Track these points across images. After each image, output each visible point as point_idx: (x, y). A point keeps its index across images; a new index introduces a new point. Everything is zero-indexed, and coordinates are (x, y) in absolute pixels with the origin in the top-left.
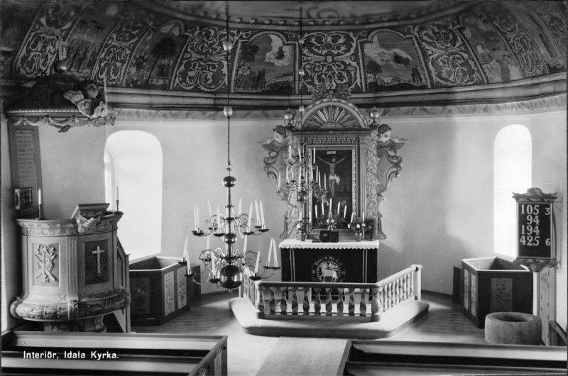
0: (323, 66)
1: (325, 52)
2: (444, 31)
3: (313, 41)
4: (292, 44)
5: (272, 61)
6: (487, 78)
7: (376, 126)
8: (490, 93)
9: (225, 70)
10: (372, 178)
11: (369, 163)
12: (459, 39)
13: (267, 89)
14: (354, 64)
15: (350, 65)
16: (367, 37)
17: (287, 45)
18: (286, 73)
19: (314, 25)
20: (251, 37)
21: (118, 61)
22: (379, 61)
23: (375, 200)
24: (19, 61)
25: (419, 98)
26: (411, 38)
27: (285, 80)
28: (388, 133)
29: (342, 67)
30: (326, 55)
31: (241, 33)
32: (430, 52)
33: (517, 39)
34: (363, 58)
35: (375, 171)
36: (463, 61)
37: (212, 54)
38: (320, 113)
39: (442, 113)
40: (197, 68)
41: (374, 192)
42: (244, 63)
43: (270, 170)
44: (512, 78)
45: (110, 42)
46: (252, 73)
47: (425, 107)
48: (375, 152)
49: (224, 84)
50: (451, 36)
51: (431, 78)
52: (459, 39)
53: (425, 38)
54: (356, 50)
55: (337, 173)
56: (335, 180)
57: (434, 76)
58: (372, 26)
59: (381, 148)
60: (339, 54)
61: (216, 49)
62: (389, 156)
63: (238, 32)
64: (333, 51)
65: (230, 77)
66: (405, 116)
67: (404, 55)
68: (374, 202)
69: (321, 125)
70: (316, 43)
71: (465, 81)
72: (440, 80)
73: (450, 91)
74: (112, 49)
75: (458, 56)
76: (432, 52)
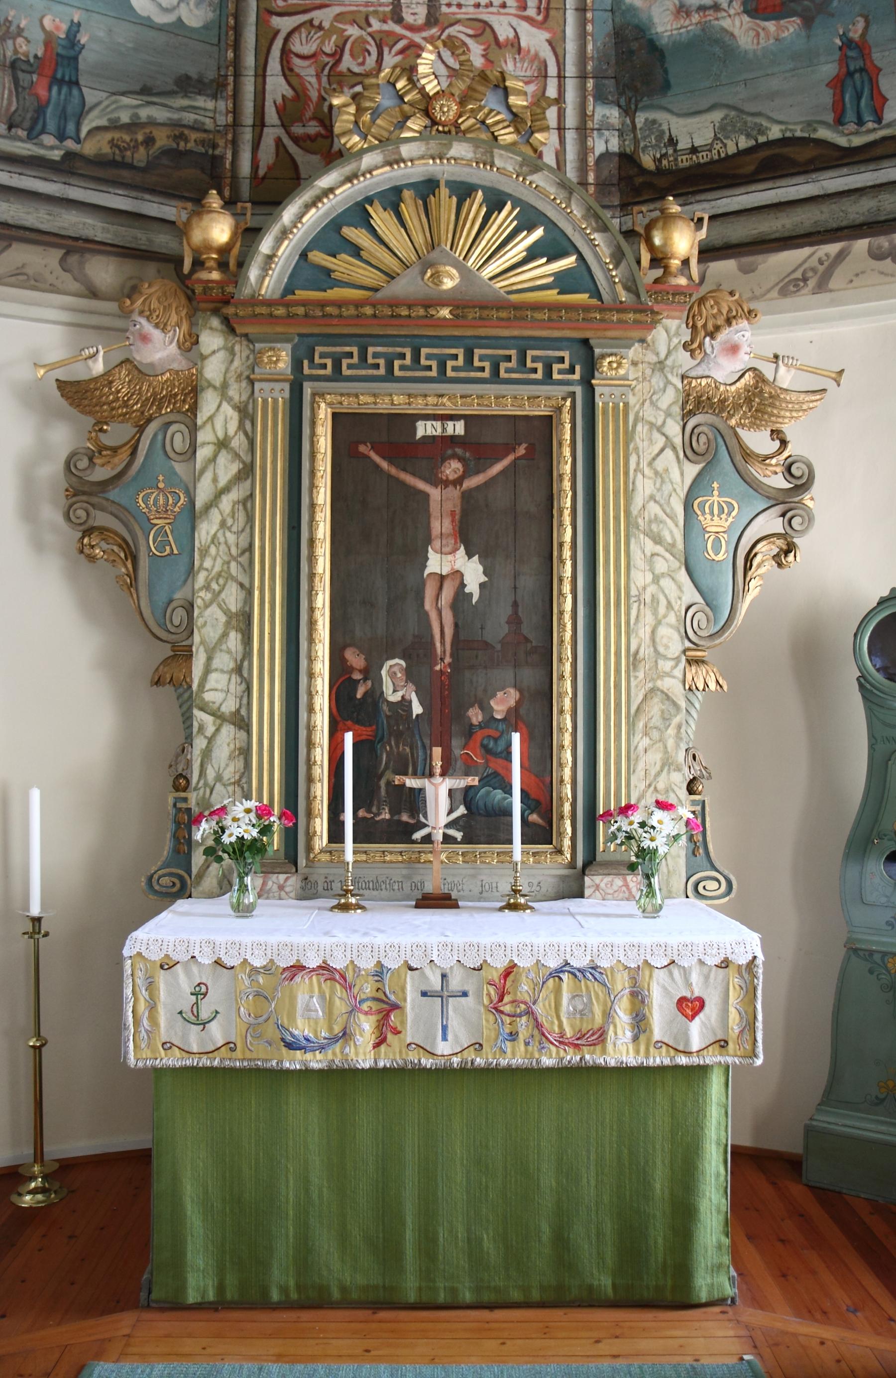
0: (382, 42)
7: (678, 292)
10: (661, 566)
11: (644, 487)
13: (89, 148)
15: (515, 45)
18: (193, 73)
23: (673, 686)
27: (189, 117)
29: (476, 55)
35: (674, 532)
38: (381, 218)
41: (673, 643)
43: (101, 519)
48: (674, 429)
56: (458, 574)
62: (748, 455)
66: (788, 301)
69: (391, 276)
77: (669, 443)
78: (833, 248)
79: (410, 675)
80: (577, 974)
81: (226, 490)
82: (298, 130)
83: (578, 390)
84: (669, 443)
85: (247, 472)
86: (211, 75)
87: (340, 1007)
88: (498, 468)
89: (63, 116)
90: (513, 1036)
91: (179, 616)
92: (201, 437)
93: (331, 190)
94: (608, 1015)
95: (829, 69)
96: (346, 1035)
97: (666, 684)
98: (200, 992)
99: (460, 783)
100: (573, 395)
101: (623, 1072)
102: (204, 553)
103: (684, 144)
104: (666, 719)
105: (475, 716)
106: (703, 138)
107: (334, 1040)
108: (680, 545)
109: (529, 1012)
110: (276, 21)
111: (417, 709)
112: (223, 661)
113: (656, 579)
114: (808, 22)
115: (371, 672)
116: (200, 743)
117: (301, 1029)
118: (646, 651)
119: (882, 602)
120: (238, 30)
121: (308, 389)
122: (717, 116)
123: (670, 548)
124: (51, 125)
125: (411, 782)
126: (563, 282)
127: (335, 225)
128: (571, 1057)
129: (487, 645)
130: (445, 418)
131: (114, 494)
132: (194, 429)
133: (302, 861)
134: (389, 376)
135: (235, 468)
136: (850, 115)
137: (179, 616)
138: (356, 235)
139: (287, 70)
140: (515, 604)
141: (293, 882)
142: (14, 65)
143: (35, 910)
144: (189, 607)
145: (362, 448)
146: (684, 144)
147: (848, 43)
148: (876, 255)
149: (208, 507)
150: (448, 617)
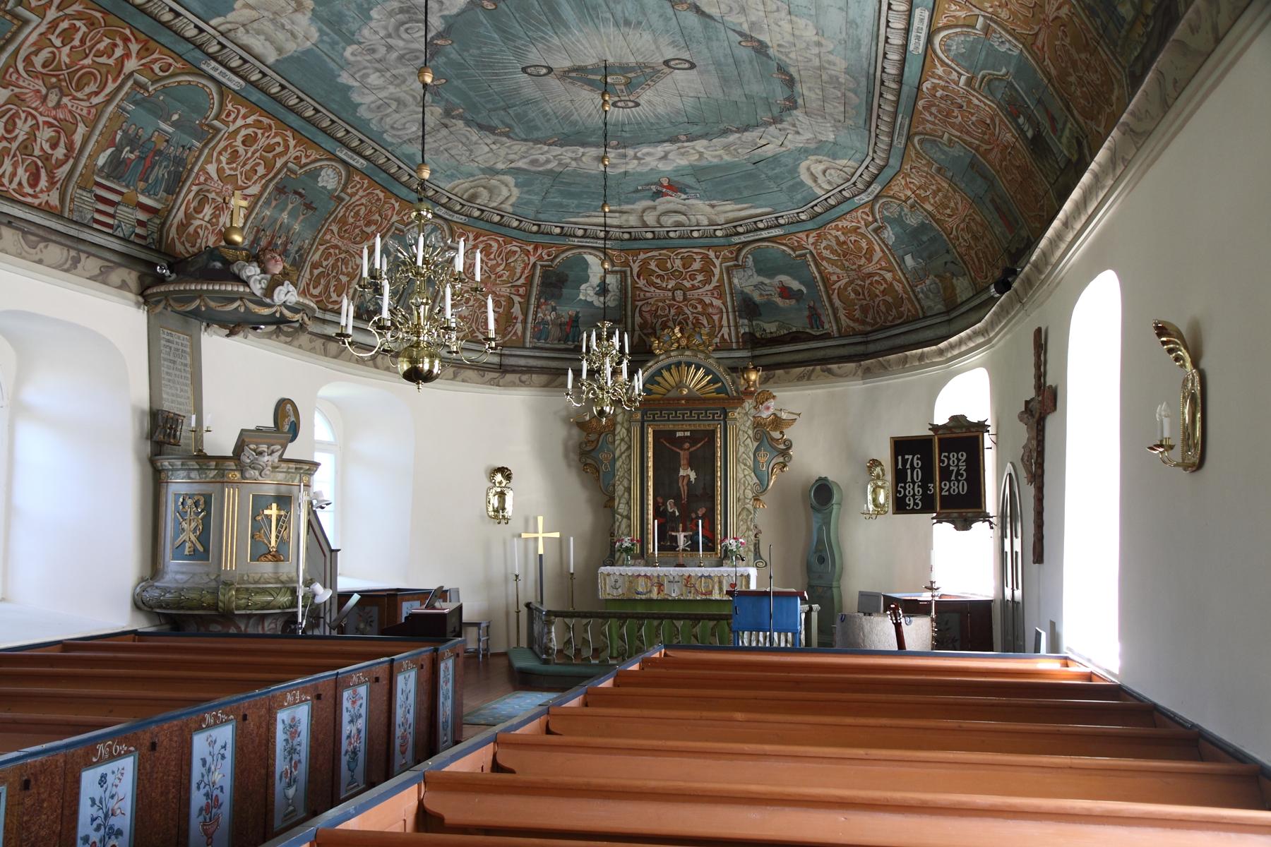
1: (671, 284)
2: (853, 239)
3: (653, 266)
4: (621, 272)
5: (589, 299)
6: (922, 308)
7: (752, 393)
8: (928, 332)
9: (516, 310)
11: (742, 449)
12: (877, 248)
14: (717, 302)
15: (711, 304)
16: (737, 259)
17: (612, 272)
19: (653, 239)
20: (556, 257)
21: (343, 273)
22: (756, 297)
23: (749, 506)
24: (173, 230)
25: (820, 354)
26: (804, 255)
28: (772, 403)
29: (700, 308)
30: (674, 290)
31: (539, 252)
32: (834, 278)
33: (962, 226)
34: (731, 294)
35: (750, 462)
36: (885, 285)
37: (495, 284)
38: (666, 374)
39: (854, 375)
40: (471, 303)
41: (750, 494)
42: (546, 300)
43: (589, 461)
44: (959, 301)
45: (328, 237)
46: (558, 317)
47: (829, 366)
48: (750, 432)
49: (515, 333)
50: (864, 244)
51: (837, 319)
52: (877, 248)
53: (826, 253)
54: (721, 280)
55: (691, 465)
57: (843, 317)
58: (743, 239)
59: (758, 425)
60: (694, 288)
61: (500, 276)
62: (773, 439)
63: (536, 249)
64: (685, 283)
65: (525, 322)
66: (800, 383)
67: (795, 285)
68: (748, 510)
69: (669, 391)
70: (657, 270)
71: (890, 318)
72: (852, 324)
73: (869, 339)
74: (332, 251)
75: (876, 278)
76: (838, 277)
77: (749, 437)
78: (811, 368)
79: (675, 504)
80: (705, 577)
81: (624, 452)
82: (645, 331)
83: (722, 423)
84: (749, 437)
85: (629, 447)
86: (618, 318)
87: (649, 585)
88: (699, 445)
89: (574, 337)
90: (690, 592)
91: (611, 488)
92: (617, 438)
93: (651, 366)
94: (713, 587)
95: (806, 313)
96: (650, 592)
97: (748, 506)
98: (616, 581)
99: (686, 534)
100: (720, 424)
101: (717, 601)
102: (618, 470)
103: (768, 331)
104: (747, 516)
105: (694, 516)
106: (773, 330)
107: (647, 592)
108: (752, 466)
109: (694, 586)
110: (637, 303)
111: (677, 514)
112: (623, 501)
113: (745, 476)
114: (798, 301)
115: (664, 504)
116: (617, 524)
117: (640, 589)
118: (742, 497)
119: (817, 481)
120: (626, 305)
121: (646, 424)
122: (777, 323)
123: (749, 467)
124: (571, 339)
125: (673, 534)
126: (718, 391)
127: (653, 376)
128: (704, 597)
129: (697, 496)
130: (684, 431)
131: (593, 454)
132: (614, 435)
133: (645, 557)
134: (669, 420)
135: (626, 446)
136: (815, 326)
137: (611, 488)
138: (659, 379)
139: (641, 315)
140: (705, 484)
141: (643, 562)
142: (560, 325)
143: (572, 571)
144: (614, 486)
145: (662, 440)
146: (768, 331)
147: (810, 307)
148: (823, 371)
149: (619, 458)
150: (686, 487)
